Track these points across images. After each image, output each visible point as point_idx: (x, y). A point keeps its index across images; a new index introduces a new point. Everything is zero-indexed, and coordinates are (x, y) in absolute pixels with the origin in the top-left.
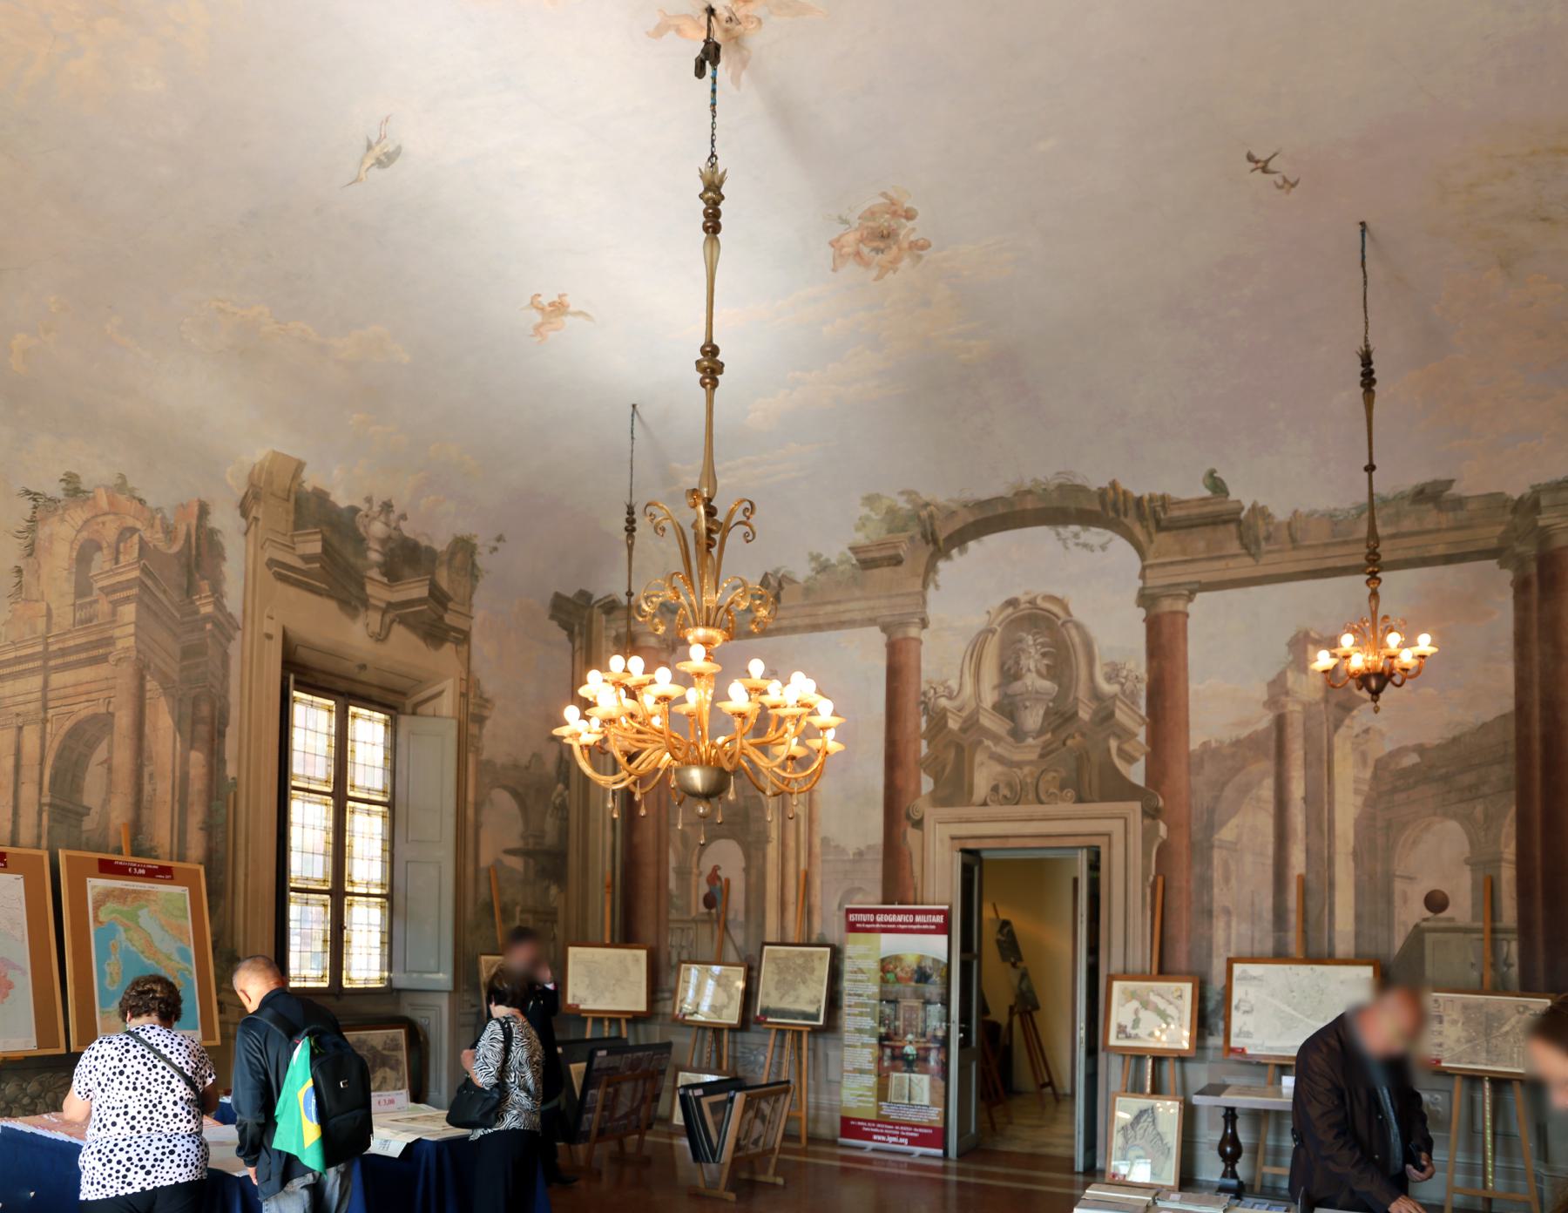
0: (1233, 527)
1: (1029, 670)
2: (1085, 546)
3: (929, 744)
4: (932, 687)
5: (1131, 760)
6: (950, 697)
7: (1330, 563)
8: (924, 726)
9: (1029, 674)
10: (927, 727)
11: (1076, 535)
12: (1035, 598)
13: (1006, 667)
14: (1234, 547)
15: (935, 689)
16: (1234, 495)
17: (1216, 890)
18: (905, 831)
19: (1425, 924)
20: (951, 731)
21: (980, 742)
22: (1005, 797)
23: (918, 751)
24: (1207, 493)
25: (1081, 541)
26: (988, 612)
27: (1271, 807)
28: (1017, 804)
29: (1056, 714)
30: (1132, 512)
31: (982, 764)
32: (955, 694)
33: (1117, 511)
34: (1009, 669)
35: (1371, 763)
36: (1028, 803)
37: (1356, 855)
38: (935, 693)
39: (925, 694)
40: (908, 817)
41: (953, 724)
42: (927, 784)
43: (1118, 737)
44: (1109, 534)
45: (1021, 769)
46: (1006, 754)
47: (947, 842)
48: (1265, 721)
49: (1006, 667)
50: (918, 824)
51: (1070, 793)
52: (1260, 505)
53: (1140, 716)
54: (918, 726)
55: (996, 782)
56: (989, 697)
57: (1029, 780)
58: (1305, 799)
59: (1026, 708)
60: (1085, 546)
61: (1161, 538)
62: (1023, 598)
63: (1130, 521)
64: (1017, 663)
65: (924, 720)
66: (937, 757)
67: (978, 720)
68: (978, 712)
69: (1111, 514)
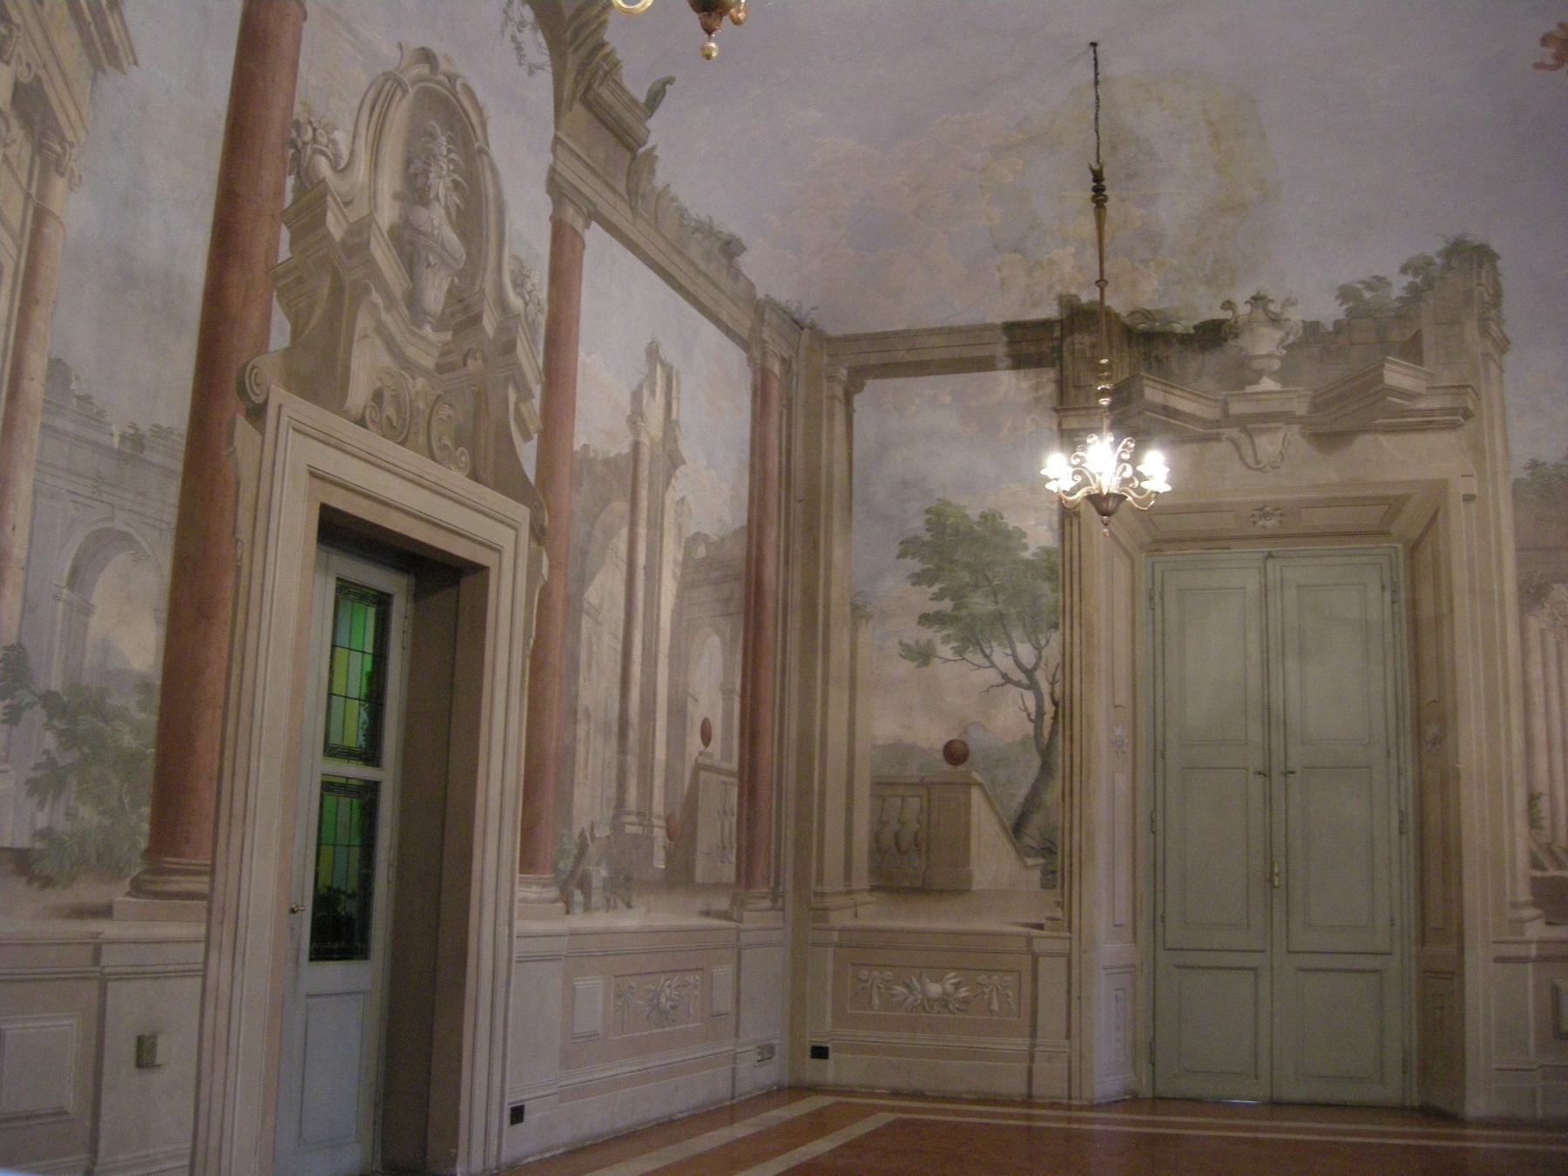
0: (628, 155)
1: (437, 198)
2: (519, 49)
3: (293, 242)
4: (310, 123)
5: (527, 437)
6: (334, 166)
7: (672, 269)
8: (289, 197)
9: (436, 204)
10: (296, 201)
11: (522, 25)
12: (457, 77)
13: (412, 170)
14: (622, 189)
15: (315, 130)
16: (652, 123)
17: (581, 679)
18: (232, 425)
19: (701, 759)
20: (327, 236)
21: (367, 290)
22: (390, 421)
23: (274, 248)
24: (642, 98)
25: (520, 37)
26: (400, 47)
27: (624, 567)
28: (403, 443)
29: (461, 301)
30: (583, 52)
31: (366, 336)
32: (340, 168)
33: (576, 35)
34: (416, 175)
35: (683, 540)
36: (415, 449)
37: (670, 657)
38: (314, 139)
39: (298, 126)
40: (242, 391)
41: (335, 226)
42: (280, 335)
43: (518, 389)
44: (544, 58)
45: (413, 378)
46: (398, 337)
47: (305, 475)
48: (625, 448)
49: (412, 170)
50: (257, 414)
51: (463, 455)
52: (656, 153)
53: (538, 368)
54: (280, 193)
55: (378, 384)
56: (387, 214)
57: (421, 405)
58: (645, 568)
59: (429, 265)
60: (519, 49)
61: (578, 108)
62: (443, 66)
63: (572, 62)
64: (426, 172)
65: (290, 181)
66: (300, 280)
67: (368, 244)
68: (370, 227)
69: (568, 35)
